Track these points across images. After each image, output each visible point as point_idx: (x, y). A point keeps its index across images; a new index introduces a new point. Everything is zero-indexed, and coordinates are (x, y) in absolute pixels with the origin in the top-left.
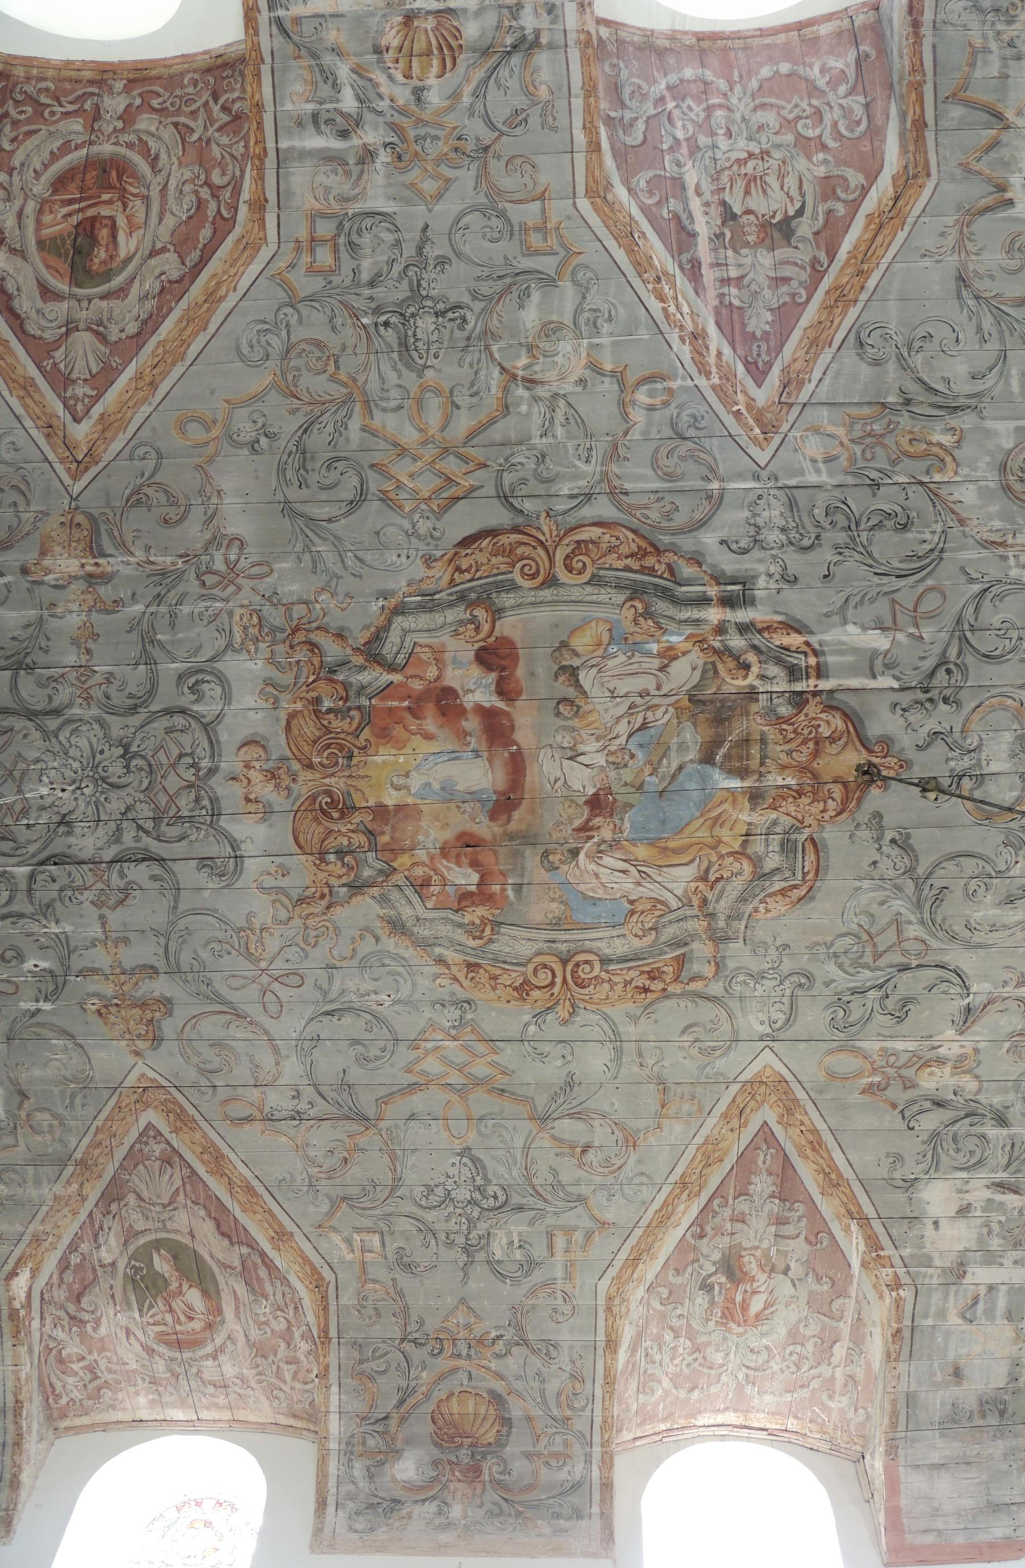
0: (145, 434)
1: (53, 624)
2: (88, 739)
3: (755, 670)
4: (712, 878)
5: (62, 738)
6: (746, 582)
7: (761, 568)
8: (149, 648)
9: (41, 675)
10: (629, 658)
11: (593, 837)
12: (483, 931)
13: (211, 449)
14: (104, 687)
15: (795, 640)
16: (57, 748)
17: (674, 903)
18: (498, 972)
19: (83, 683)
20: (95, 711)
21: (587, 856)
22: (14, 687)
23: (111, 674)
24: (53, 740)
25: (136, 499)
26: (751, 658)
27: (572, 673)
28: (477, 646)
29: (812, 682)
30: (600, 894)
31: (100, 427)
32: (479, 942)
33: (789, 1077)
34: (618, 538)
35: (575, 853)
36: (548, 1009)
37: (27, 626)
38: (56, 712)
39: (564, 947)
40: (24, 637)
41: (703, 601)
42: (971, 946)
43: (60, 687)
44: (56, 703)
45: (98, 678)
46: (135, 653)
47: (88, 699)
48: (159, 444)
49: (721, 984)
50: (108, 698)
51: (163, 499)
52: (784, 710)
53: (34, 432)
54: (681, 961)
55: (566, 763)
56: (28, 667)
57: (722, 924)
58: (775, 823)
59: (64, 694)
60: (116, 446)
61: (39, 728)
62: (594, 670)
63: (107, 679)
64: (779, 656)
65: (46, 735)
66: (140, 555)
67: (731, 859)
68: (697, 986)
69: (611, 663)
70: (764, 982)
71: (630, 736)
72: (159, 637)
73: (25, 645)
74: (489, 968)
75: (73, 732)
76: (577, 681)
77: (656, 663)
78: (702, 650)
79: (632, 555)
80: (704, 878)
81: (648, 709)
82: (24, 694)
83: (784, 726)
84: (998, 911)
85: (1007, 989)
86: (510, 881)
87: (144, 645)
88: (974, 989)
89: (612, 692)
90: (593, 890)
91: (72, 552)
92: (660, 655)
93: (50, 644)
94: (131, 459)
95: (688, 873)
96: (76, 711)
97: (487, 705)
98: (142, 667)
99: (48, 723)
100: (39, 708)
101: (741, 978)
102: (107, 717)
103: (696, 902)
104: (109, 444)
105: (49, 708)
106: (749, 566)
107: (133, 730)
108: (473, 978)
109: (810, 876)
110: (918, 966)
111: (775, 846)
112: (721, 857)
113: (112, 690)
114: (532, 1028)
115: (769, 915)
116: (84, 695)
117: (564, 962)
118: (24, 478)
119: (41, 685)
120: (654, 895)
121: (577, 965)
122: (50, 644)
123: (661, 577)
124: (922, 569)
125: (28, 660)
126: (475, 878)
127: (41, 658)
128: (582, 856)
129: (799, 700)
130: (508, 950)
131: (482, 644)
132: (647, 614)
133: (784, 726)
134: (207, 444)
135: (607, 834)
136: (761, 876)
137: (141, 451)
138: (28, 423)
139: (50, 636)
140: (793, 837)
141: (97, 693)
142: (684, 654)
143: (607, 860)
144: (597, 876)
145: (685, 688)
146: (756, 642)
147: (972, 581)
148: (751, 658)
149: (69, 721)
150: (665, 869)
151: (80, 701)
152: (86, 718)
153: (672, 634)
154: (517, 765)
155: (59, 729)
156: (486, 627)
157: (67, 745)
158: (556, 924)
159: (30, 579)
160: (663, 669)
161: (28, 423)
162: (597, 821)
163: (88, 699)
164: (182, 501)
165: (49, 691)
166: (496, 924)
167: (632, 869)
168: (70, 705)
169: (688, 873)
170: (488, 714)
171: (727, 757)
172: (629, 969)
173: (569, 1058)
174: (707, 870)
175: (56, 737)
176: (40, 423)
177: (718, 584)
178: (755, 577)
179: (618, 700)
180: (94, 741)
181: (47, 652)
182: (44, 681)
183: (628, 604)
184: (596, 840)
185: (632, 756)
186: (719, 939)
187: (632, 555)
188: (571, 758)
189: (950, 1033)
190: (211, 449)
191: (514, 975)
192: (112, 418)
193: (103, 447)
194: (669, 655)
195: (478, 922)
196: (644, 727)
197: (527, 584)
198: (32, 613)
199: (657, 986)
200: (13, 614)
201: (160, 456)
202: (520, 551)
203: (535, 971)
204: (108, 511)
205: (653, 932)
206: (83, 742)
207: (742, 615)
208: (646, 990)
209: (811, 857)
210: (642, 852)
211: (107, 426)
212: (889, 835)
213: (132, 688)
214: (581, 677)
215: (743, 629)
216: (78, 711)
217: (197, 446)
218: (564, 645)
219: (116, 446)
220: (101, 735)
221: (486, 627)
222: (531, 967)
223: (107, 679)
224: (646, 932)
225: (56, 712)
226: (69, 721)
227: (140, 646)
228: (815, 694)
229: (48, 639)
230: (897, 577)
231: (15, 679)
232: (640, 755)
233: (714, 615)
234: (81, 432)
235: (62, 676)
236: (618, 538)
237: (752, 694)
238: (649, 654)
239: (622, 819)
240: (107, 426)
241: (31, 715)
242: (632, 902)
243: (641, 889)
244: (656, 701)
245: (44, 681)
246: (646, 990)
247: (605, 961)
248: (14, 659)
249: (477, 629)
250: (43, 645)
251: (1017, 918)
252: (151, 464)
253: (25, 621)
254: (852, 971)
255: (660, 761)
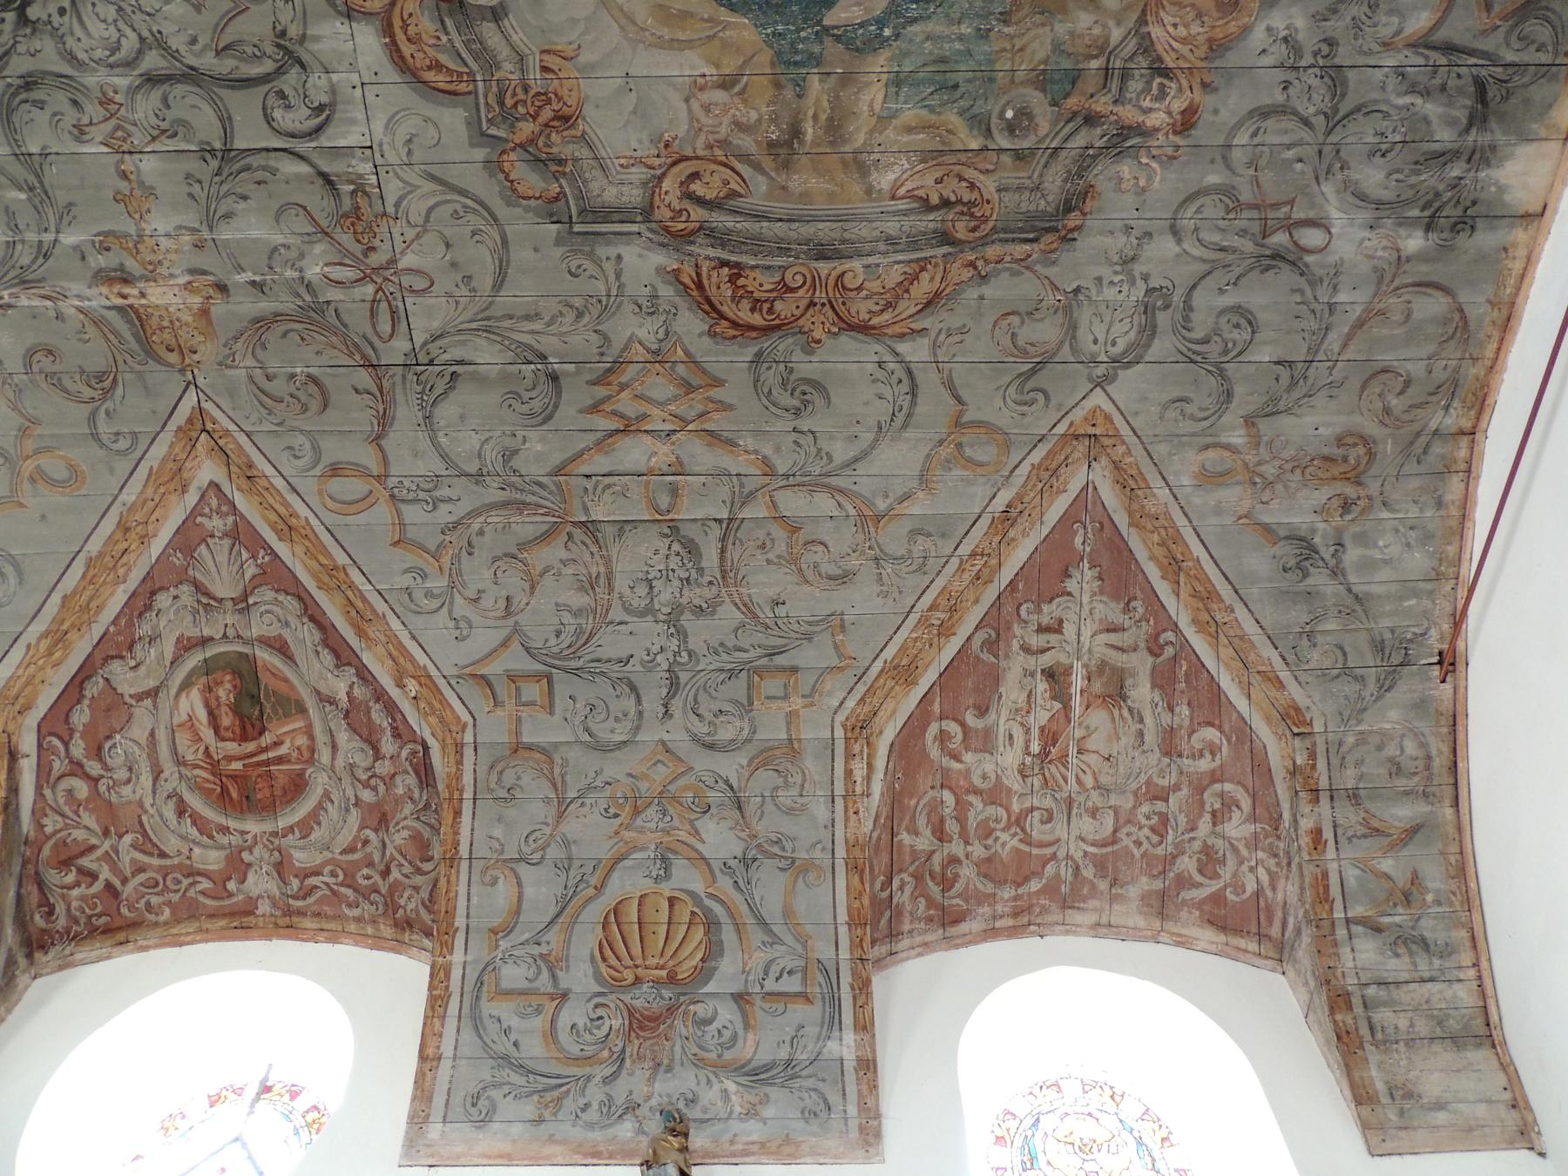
0: (124, 466)
1: (191, 218)
2: (89, 34)
5: (133, 36)
8: (32, 179)
9: (188, 141)
13: (30, 445)
14: (86, 120)
16: (138, 18)
19: (118, 128)
20: (91, 80)
22: (226, 122)
23: (78, 140)
24: (146, 33)
25: (105, 383)
31: (185, 475)
37: (228, 216)
38: (152, 80)
40: (230, 200)
43: (154, 121)
44: (156, 94)
45: (99, 133)
46: (52, 173)
47: (105, 101)
48: (102, 453)
50: (75, 102)
51: (66, 382)
53: (269, 471)
56: (212, 152)
59: (146, 107)
60: (159, 450)
61: (174, 55)
63: (83, 133)
65: (160, 42)
66: (68, 307)
72: (23, 196)
73: (225, 188)
75: (116, 49)
82: (208, 109)
87: (41, 183)
91: (164, 314)
93: (187, 189)
94: (134, 435)
96: (122, 82)
98: (34, 149)
99: (163, 63)
100: (179, 89)
102: (68, 71)
104: (169, 453)
105: (166, 87)
107: (21, 48)
113: (71, 116)
116: (113, 107)
118: (270, 413)
119: (183, 123)
122: (187, 189)
125: (214, 164)
127: (193, 165)
134: (37, 452)
137: (123, 444)
138: (279, 483)
139: (191, 202)
141: (93, 110)
149: (129, 64)
151: (119, 98)
152: (103, 71)
155: (140, 52)
157: (121, 24)
159: (210, 278)
161: (279, 483)
163: (105, 101)
164: (40, 378)
165: (170, 115)
168: (133, 91)
175: (142, 39)
176: (264, 482)
180: (79, 32)
181: (188, 176)
182: (181, 130)
190: (30, 445)
192: (172, 487)
193: (177, 450)
198: (226, 234)
200: (255, 234)
201: (96, 437)
204: (138, 368)
206: (96, 28)
211: (174, 477)
213: (42, 117)
216: (117, 81)
217: (48, 449)
219: (159, 450)
220: (70, 42)
223: (83, 133)
225: (152, 80)
226: (129, 64)
227: (46, 182)
229: (191, 195)
231: (227, 135)
234: (207, 471)
235: (154, 139)
240: (174, 477)
241: (192, 76)
245: (181, 130)
248: (237, 166)
250: (197, 187)
252: (104, 428)
253: (234, 223)
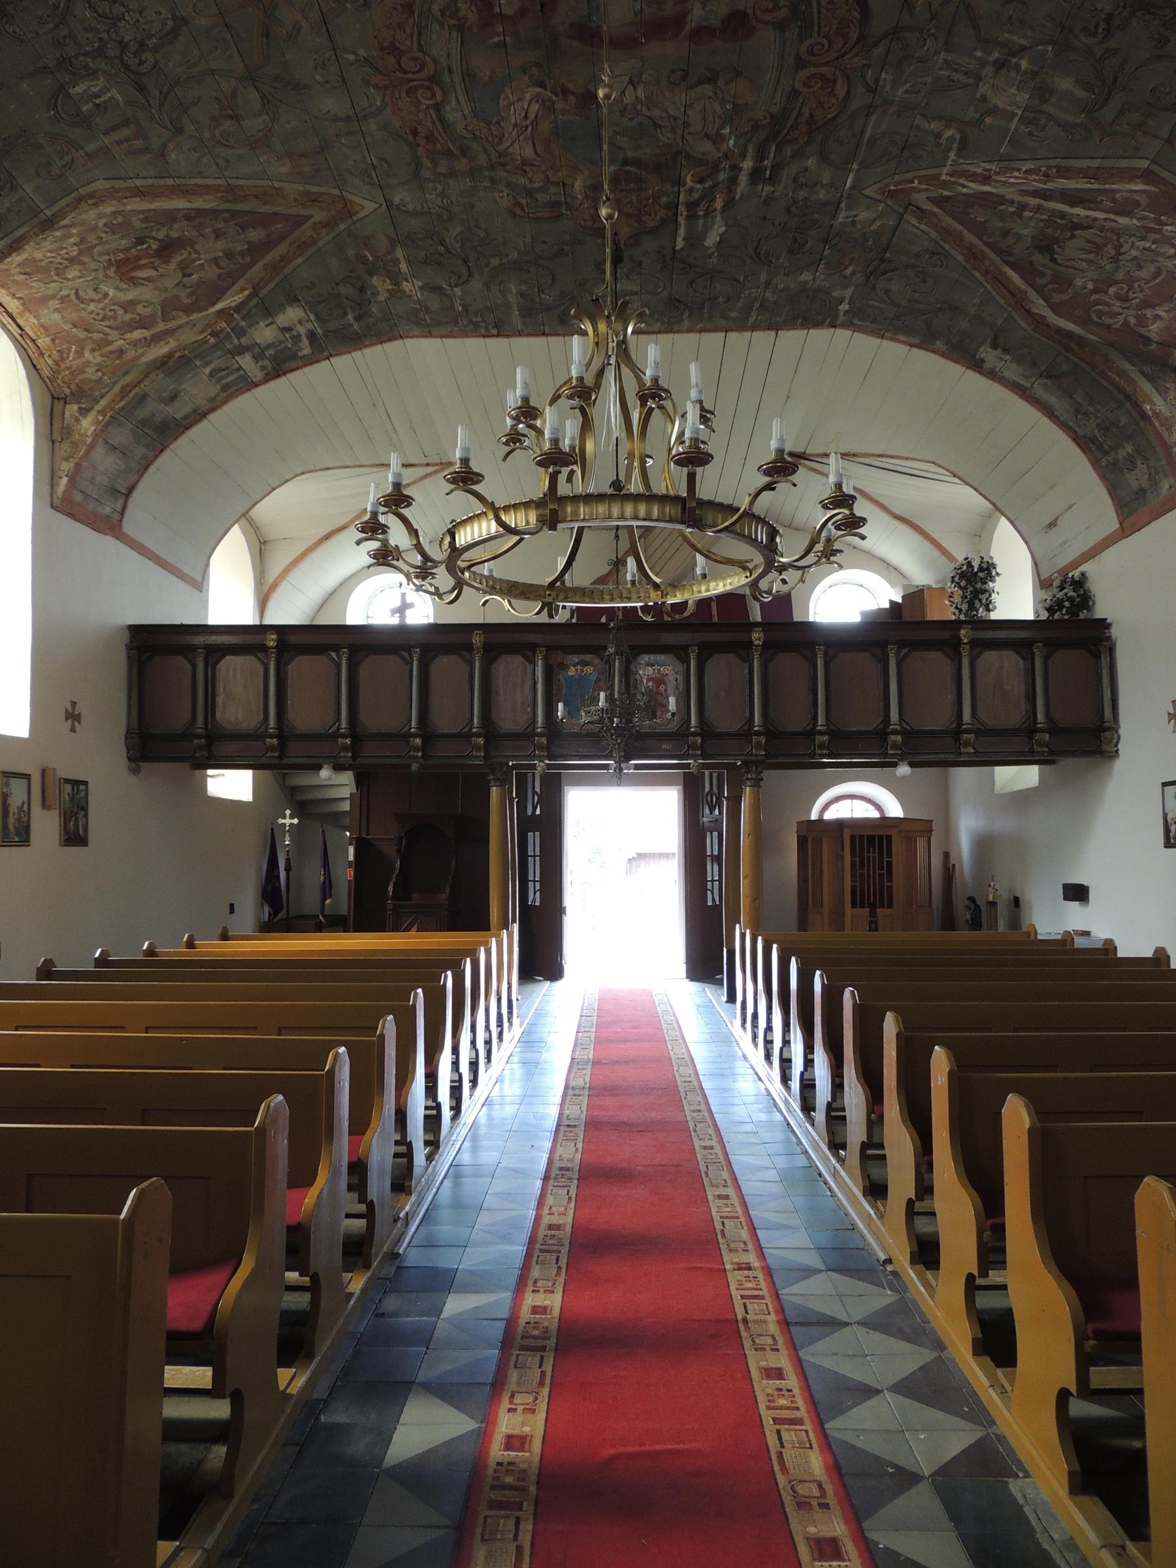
3: (699, 186)
4: (527, 168)
6: (773, 179)
7: (781, 188)
10: (720, 117)
11: (557, 96)
12: (451, 17)
15: (719, 204)
17: (501, 148)
18: (408, 30)
21: (538, 93)
26: (708, 184)
27: (712, 79)
28: (750, 12)
29: (685, 213)
30: (503, 103)
32: (439, 14)
33: (355, 218)
34: (829, 108)
35: (542, 85)
36: (377, 69)
39: (446, 78)
41: (760, 156)
42: (487, 285)
49: (432, 177)
52: (664, 199)
54: (449, 154)
55: (627, 78)
57: (487, 174)
58: (574, 198)
62: (712, 94)
64: (708, 196)
67: (542, 177)
68: (427, 163)
69: (717, 106)
70: (439, 199)
71: (649, 117)
74: (411, 22)
76: (704, 83)
77: (712, 130)
78: (719, 158)
79: (811, 117)
80: (525, 162)
81: (673, 128)
83: (651, 201)
84: (514, 291)
85: (459, 301)
86: (507, 38)
88: (455, 289)
89: (691, 106)
90: (507, 97)
92: (718, 134)
95: (529, 152)
97: (688, 19)
101: (439, 187)
103: (503, 160)
106: (783, 182)
108: (396, 9)
109: (532, 215)
110: (469, 267)
111: (553, 198)
112: (545, 172)
114: (351, 57)
115: (498, 199)
117: (431, 79)
120: (506, 135)
121: (428, 88)
123: (787, 134)
124: (760, 259)
126: (508, 11)
128: (538, 90)
129: (673, 206)
130: (434, 37)
131: (751, 16)
132: (756, 127)
133: (651, 201)
135: (559, 105)
136: (530, 193)
140: (564, 207)
142: (718, 149)
143: (535, 107)
144: (521, 100)
145: (688, 149)
146: (720, 186)
147: (746, 277)
148: (708, 184)
150: (530, 142)
153: (735, 142)
154: (625, 44)
156: (768, 17)
158: (469, 76)
160: (707, 136)
162: (573, 99)
166: (461, 29)
167: (529, 121)
169: (529, 152)
170: (679, 20)
171: (628, 173)
172: (433, 122)
173: (328, 86)
174: (533, 165)
177: (772, 167)
178: (773, 185)
179: (682, 110)
183: (768, 115)
184: (554, 98)
185: (632, 119)
186: (473, 173)
187: (811, 117)
188: (631, 81)
189: (420, 284)
191: (408, 42)
194: (718, 139)
195: (461, 14)
196: (656, 126)
197: (804, 46)
199: (421, 140)
202: (840, 41)
203: (415, 59)
205: (472, 136)
207: (743, 179)
208: (415, 134)
209: (547, 215)
210: (545, 127)
212: (567, 248)
214: (707, 86)
215: (733, 181)
218: (738, 74)
221: (768, 17)
222: (419, 55)
224: (472, 132)
228: (676, 214)
230: (756, 249)
232: (633, 124)
233: (747, 164)
236: (829, 108)
237: (680, 183)
238: (722, 126)
239: (574, 114)
242: (498, 123)
243: (511, 127)
244: (679, 132)
246: (415, 134)
247: (438, 107)
249: (767, 11)
251: (511, 300)
254: (459, 238)
255: (627, 136)
